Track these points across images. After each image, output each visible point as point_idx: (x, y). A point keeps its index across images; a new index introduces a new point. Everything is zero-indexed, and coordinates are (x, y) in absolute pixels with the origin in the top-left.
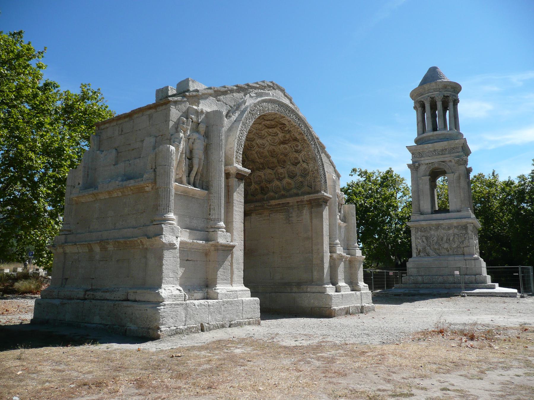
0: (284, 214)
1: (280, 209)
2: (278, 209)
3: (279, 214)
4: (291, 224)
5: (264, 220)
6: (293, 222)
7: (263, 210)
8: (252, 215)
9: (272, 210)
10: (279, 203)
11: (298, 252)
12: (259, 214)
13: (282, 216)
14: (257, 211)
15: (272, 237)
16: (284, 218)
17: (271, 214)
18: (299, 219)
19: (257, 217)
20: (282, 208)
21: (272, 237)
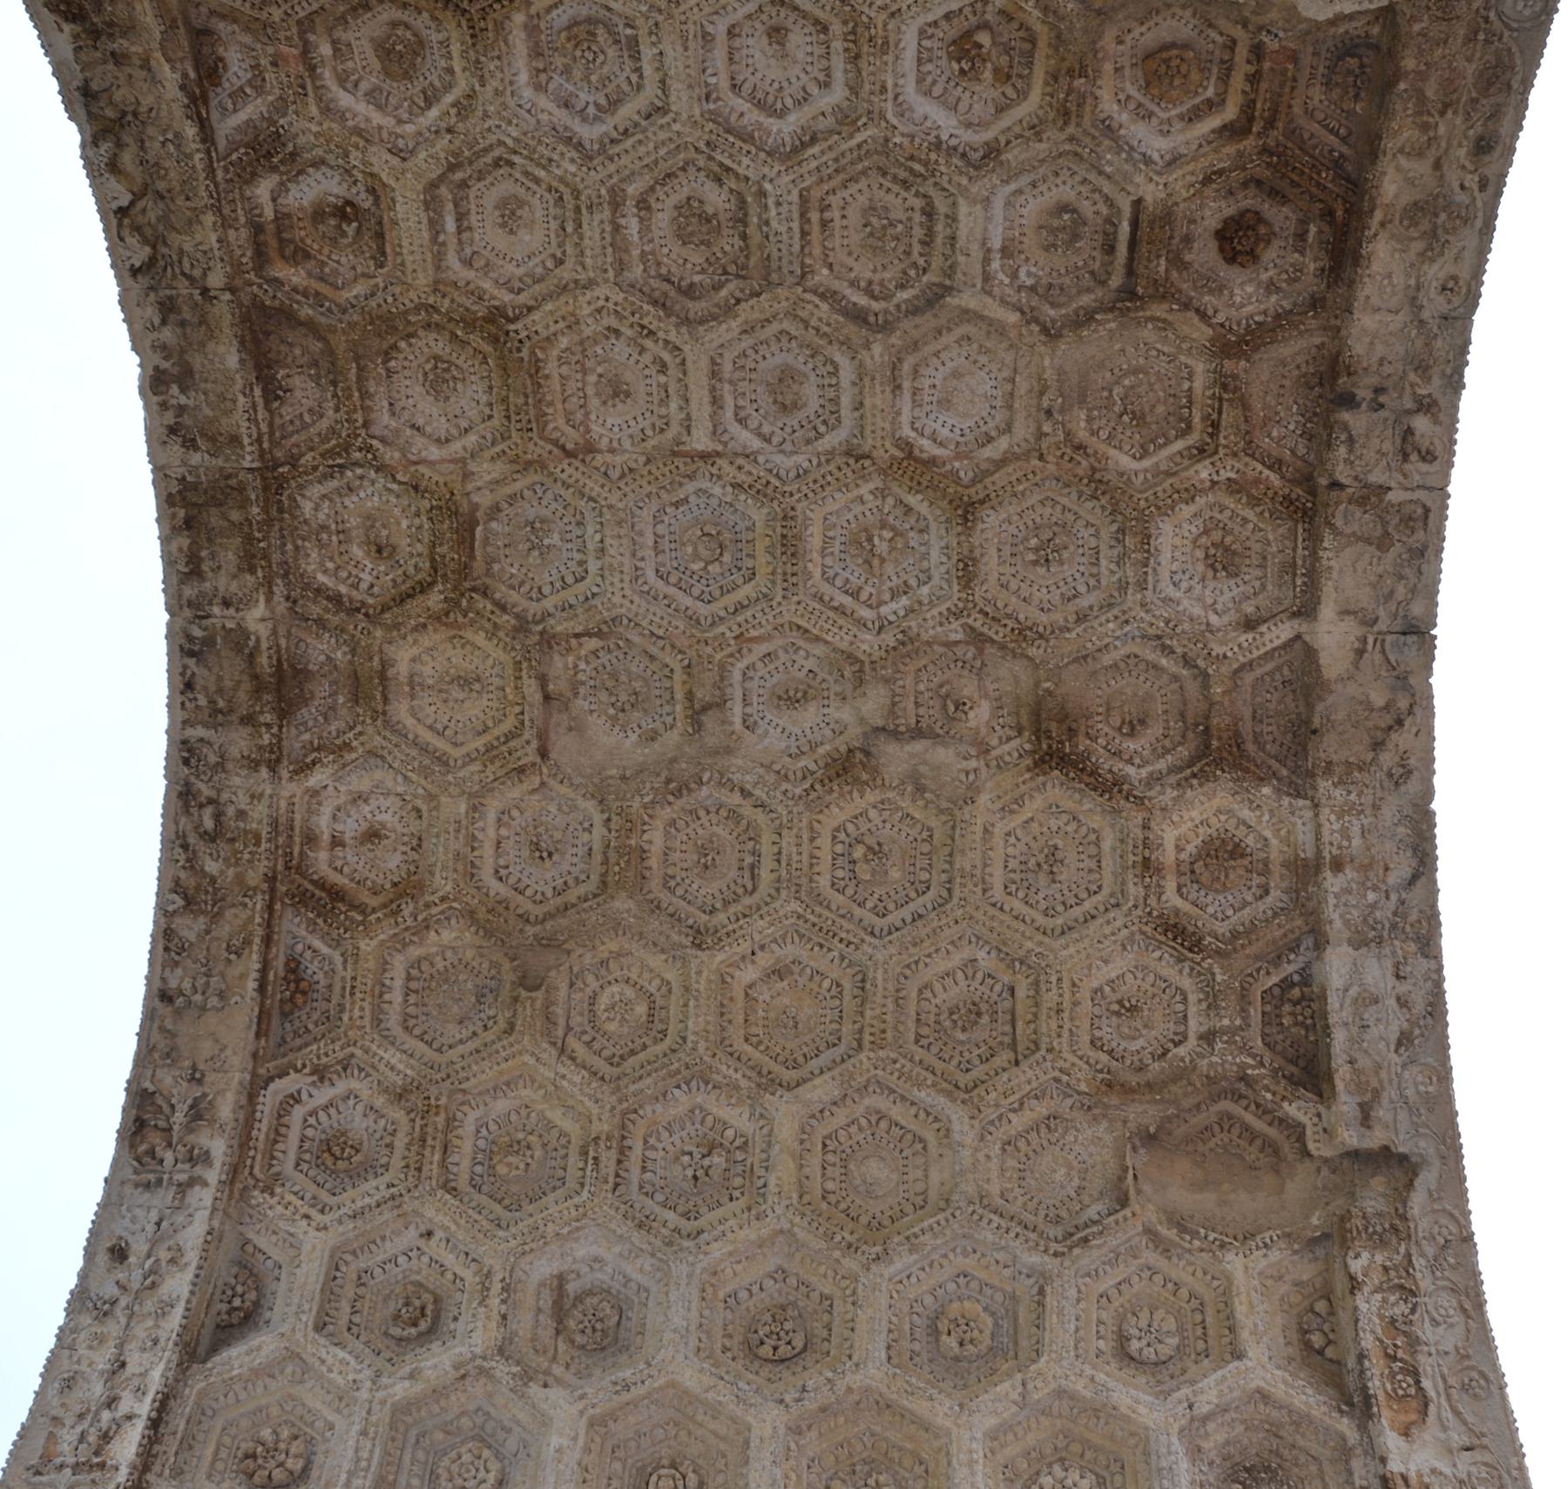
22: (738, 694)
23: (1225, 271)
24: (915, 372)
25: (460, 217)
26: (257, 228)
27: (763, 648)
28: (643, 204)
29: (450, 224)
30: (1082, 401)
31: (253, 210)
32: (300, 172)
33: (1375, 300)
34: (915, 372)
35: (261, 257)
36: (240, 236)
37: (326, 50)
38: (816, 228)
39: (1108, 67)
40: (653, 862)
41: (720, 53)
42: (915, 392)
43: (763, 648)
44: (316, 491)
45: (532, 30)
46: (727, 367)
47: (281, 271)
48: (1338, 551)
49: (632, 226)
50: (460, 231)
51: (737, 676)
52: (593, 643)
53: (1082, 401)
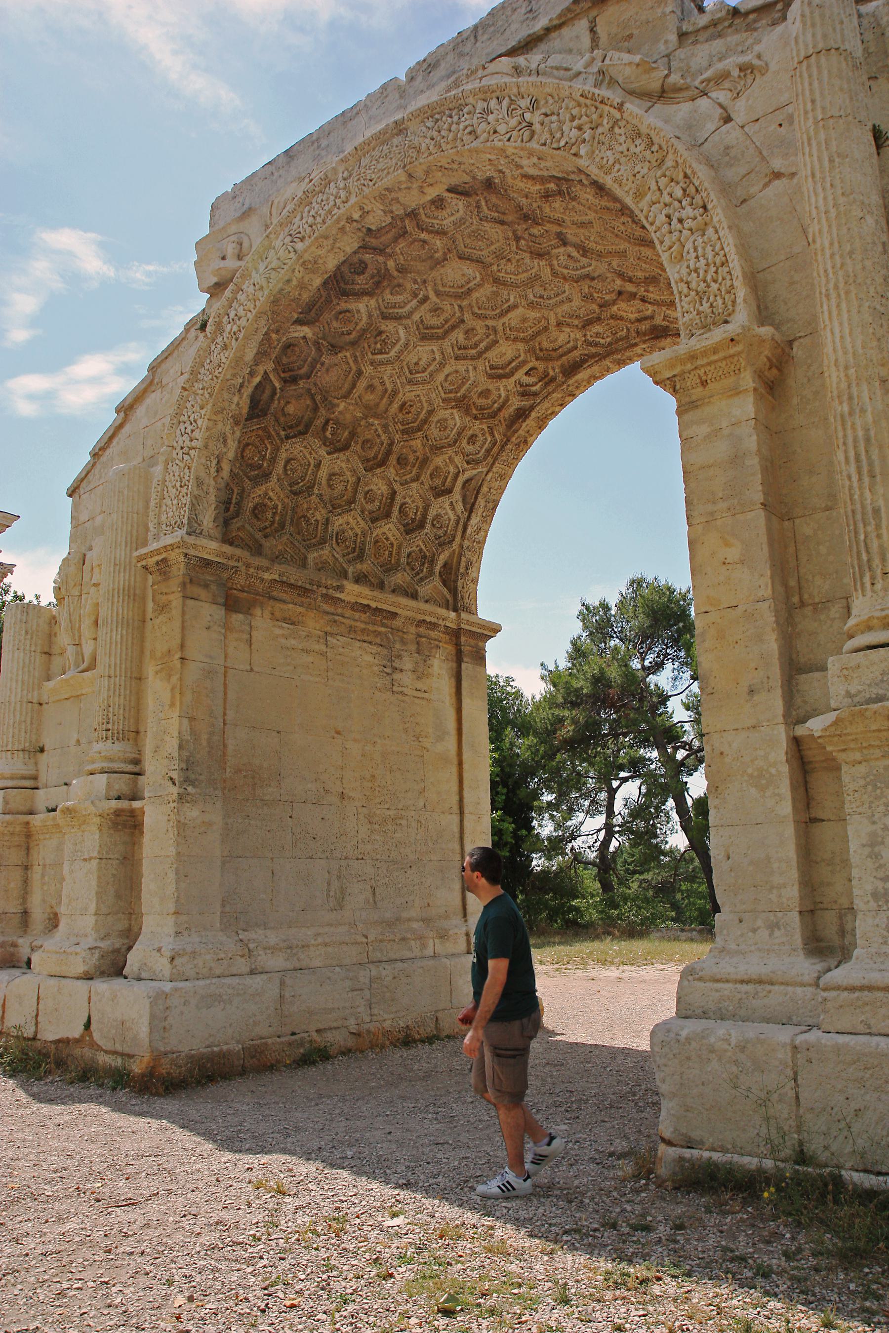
0: (375, 649)
1: (363, 626)
2: (358, 624)
3: (358, 644)
4: (400, 697)
5: (308, 652)
6: (405, 690)
7: (301, 609)
8: (258, 611)
9: (335, 621)
10: (365, 602)
11: (422, 804)
12: (285, 620)
13: (368, 658)
14: (282, 606)
15: (338, 733)
16: (376, 668)
17: (332, 634)
18: (419, 685)
19: (278, 631)
20: (371, 627)
21: (338, 733)
22: (583, 270)
23: (369, 262)
24: (462, 287)
25: (510, 363)
26: (547, 384)
27: (565, 271)
28: (476, 345)
29: (513, 364)
30: (431, 257)
31: (542, 389)
32: (527, 385)
33: (342, 254)
34: (462, 287)
35: (553, 379)
36: (550, 388)
37: (496, 405)
38: (449, 324)
39: (358, 328)
40: (647, 275)
41: (432, 368)
42: (468, 283)
43: (565, 271)
44: (602, 341)
45: (459, 388)
46: (498, 311)
47: (551, 373)
48: (410, 207)
49: (482, 345)
50: (513, 360)
51: (578, 272)
52: (595, 295)
53: (431, 257)
